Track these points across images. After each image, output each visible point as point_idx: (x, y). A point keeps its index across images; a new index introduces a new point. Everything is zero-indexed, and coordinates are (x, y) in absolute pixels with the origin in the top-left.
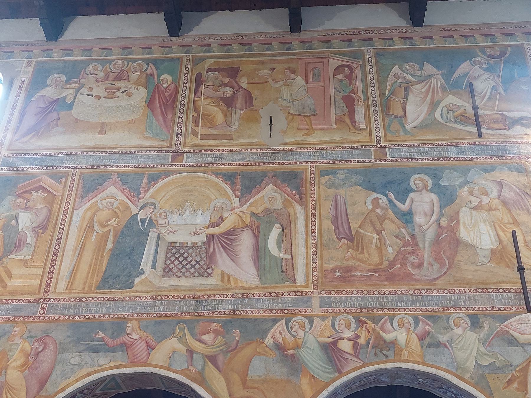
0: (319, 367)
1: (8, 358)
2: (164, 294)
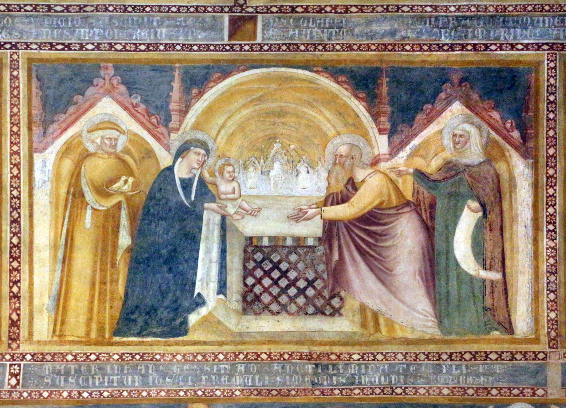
2: (251, 349)
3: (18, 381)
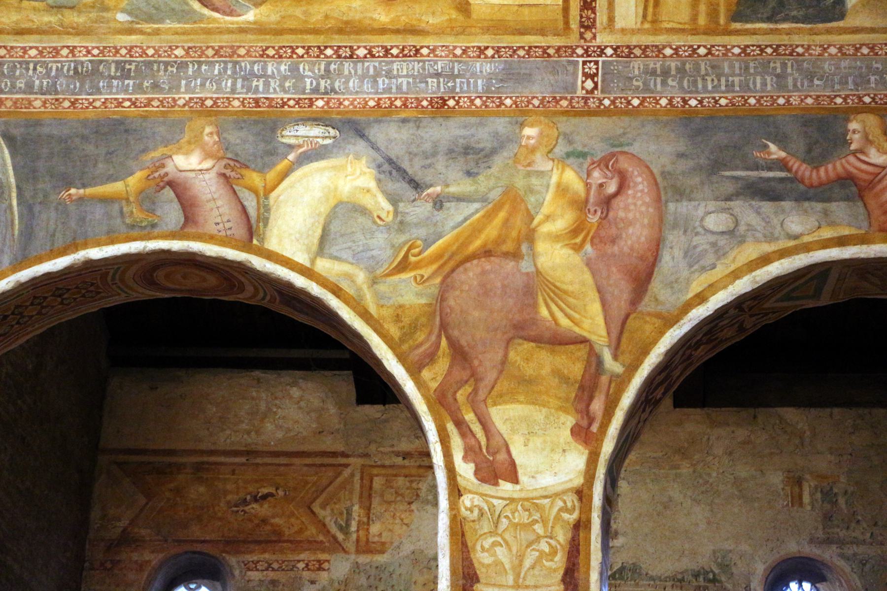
1: (528, 210)
3: (596, 84)
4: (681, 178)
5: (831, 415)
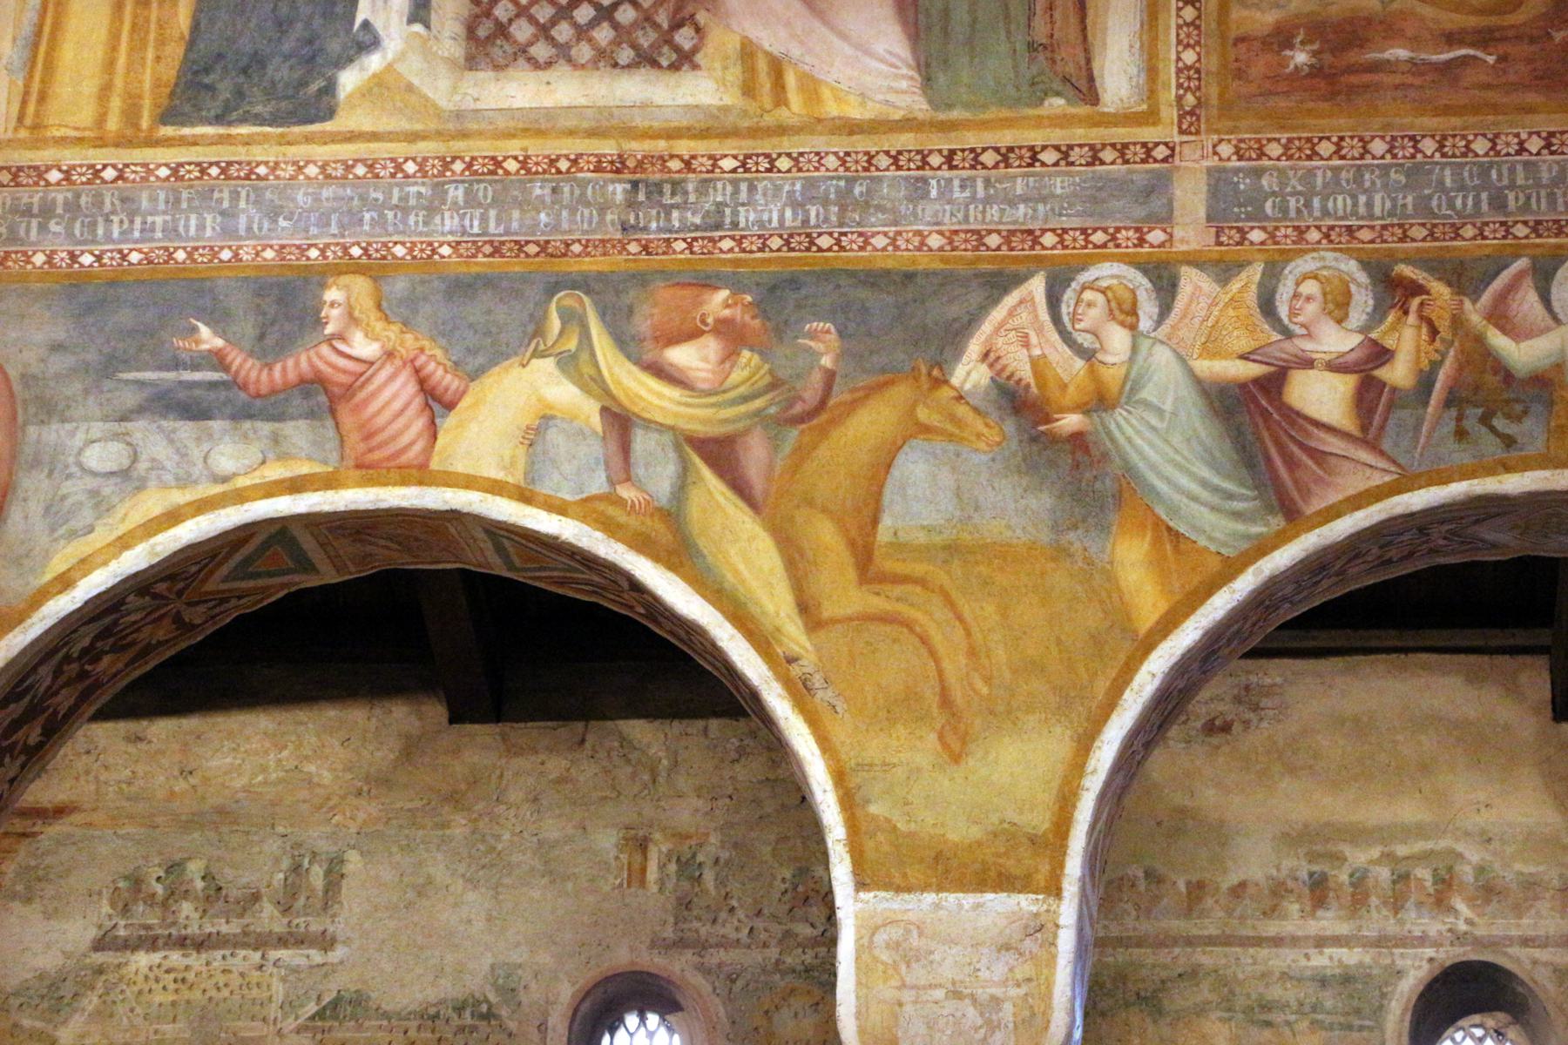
0: (1195, 488)
2: (482, 148)
4: (52, 384)
5: (706, 730)
